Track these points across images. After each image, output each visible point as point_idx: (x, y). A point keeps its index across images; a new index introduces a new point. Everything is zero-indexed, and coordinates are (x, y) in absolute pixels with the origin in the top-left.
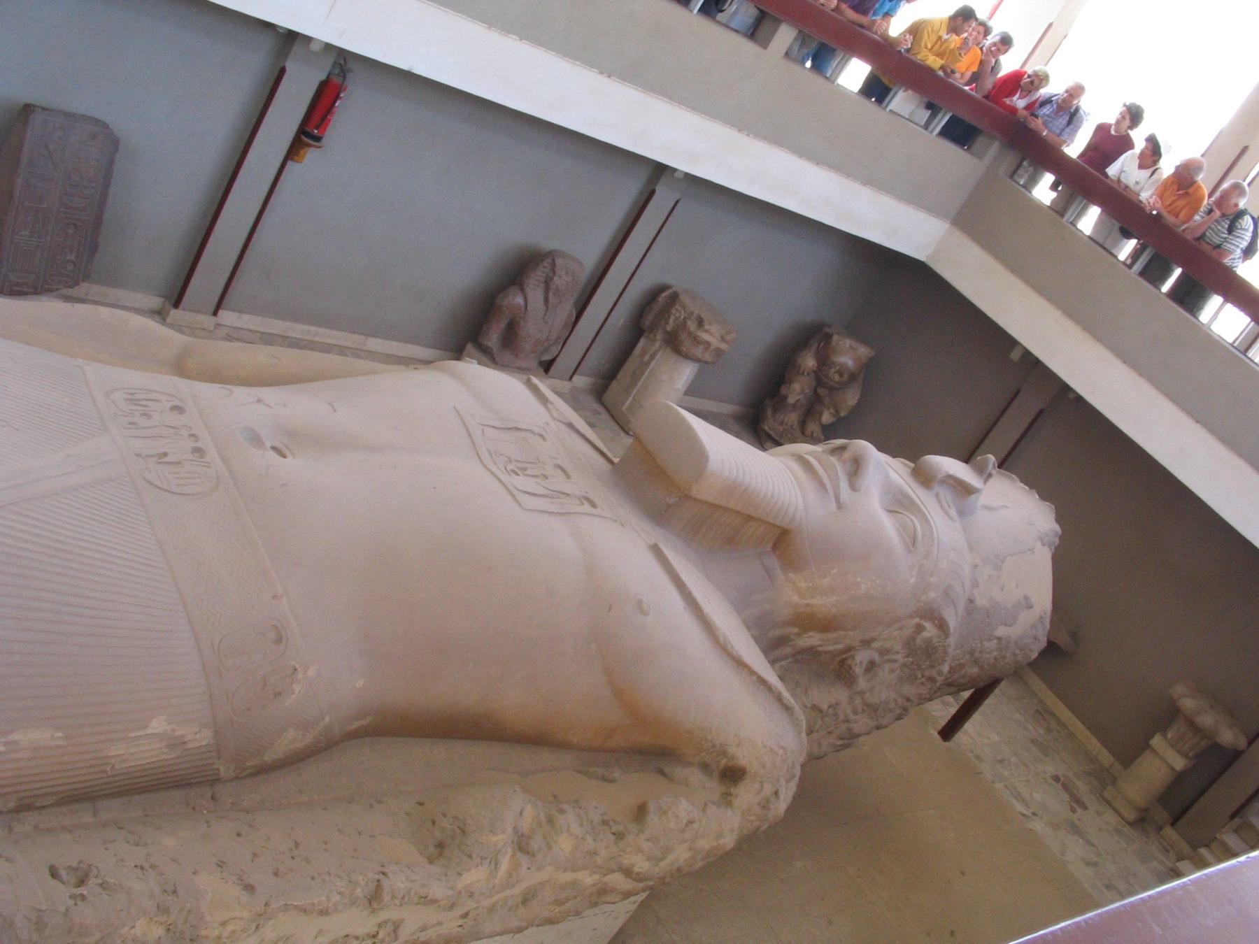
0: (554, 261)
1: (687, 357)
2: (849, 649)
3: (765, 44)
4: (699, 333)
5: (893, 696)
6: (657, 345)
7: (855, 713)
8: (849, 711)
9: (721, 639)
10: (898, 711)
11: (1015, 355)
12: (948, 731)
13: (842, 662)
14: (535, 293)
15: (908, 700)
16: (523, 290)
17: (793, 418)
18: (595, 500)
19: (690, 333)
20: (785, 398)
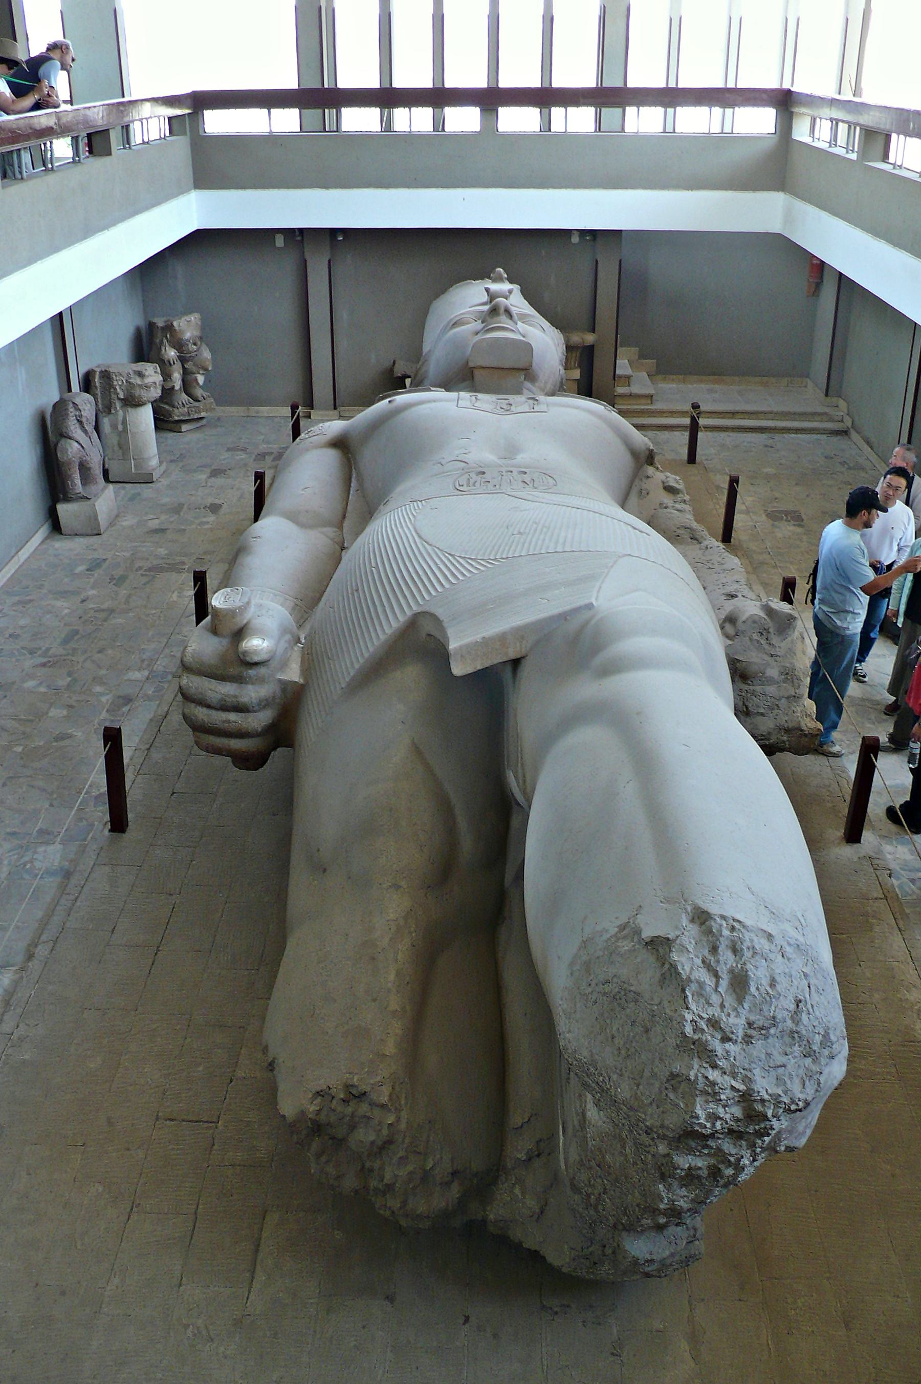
3: (109, 153)
6: (121, 413)
11: (280, 241)
14: (78, 433)
16: (70, 438)
17: (184, 397)
20: (173, 387)
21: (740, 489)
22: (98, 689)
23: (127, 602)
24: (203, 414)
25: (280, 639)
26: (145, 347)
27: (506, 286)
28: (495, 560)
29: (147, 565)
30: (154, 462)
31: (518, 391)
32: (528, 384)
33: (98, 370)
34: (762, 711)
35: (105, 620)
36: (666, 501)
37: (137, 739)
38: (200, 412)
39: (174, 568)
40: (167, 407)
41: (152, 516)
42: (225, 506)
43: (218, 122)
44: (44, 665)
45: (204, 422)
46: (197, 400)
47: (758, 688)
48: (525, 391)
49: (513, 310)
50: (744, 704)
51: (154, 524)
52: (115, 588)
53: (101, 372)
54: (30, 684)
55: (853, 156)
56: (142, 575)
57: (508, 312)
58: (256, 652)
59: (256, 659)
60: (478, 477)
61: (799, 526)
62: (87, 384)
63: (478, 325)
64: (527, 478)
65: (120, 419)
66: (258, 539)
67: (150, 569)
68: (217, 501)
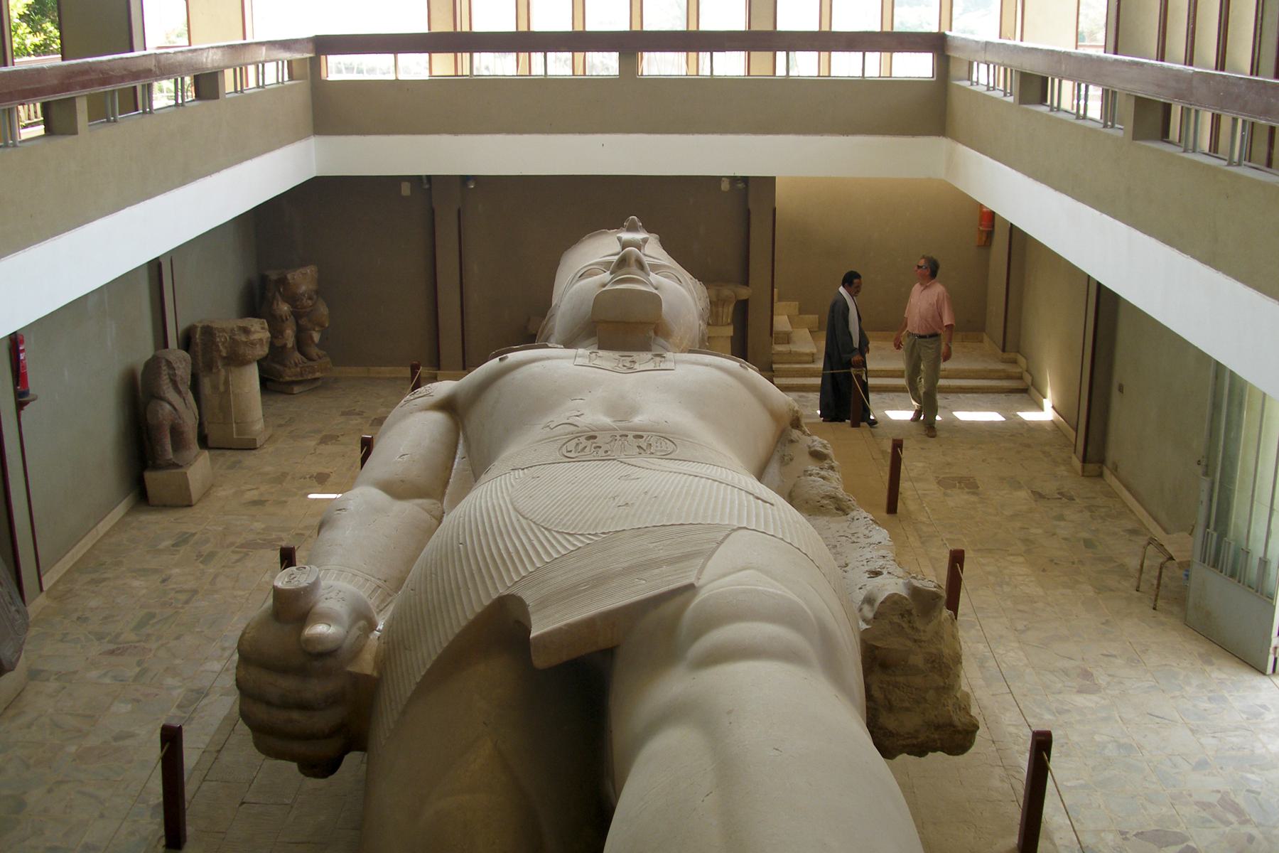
6: (223, 372)
11: (406, 189)
14: (171, 394)
17: (297, 356)
20: (284, 346)
21: (905, 455)
22: (169, 681)
23: (213, 582)
24: (318, 375)
25: (351, 627)
26: (256, 300)
27: (639, 236)
28: (595, 535)
29: (239, 541)
30: (259, 426)
31: (645, 347)
32: (662, 341)
33: (200, 325)
34: (907, 704)
35: (187, 602)
36: (810, 467)
37: (207, 739)
38: (314, 372)
39: (268, 544)
40: (278, 367)
41: (249, 487)
42: (333, 476)
43: (338, 68)
44: (112, 652)
45: (319, 383)
46: (310, 359)
47: (901, 679)
48: (654, 347)
49: (646, 260)
50: (886, 697)
51: (252, 495)
52: (202, 566)
53: (203, 328)
54: (94, 674)
55: (1010, 99)
56: (233, 552)
57: (641, 265)
58: (320, 639)
59: (320, 648)
60: (588, 443)
61: (974, 493)
62: (187, 342)
63: (606, 276)
64: (642, 443)
65: (222, 378)
66: (343, 513)
67: (242, 546)
68: (326, 471)
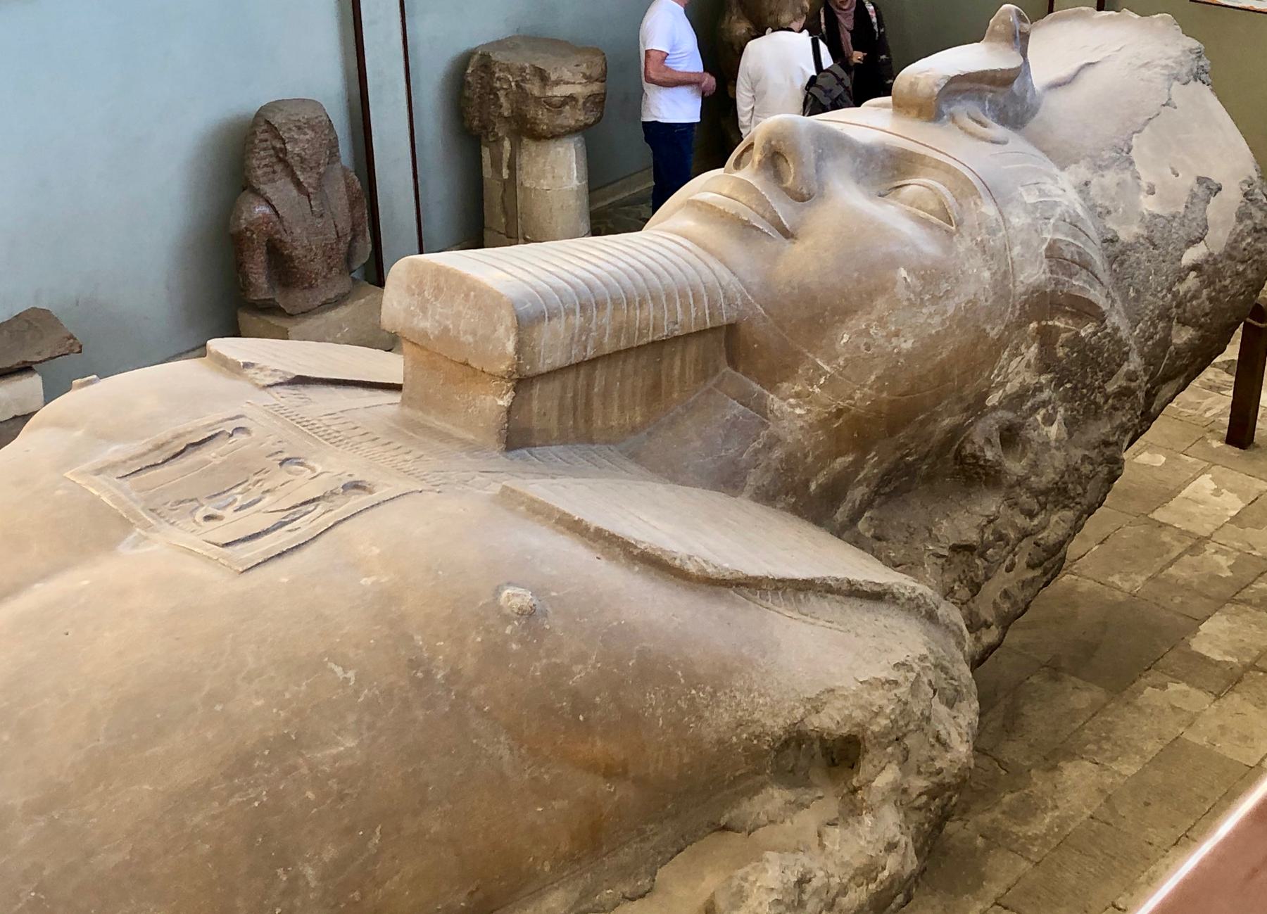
0: (268, 122)
1: (555, 136)
2: (956, 433)
4: (550, 94)
5: (1078, 453)
6: (507, 144)
7: (1031, 515)
8: (1021, 521)
9: (691, 568)
10: (1103, 471)
12: (1241, 431)
13: (959, 458)
15: (1106, 444)
16: (256, 192)
18: (368, 478)
19: (537, 99)
53: (483, 55)
65: (506, 155)
